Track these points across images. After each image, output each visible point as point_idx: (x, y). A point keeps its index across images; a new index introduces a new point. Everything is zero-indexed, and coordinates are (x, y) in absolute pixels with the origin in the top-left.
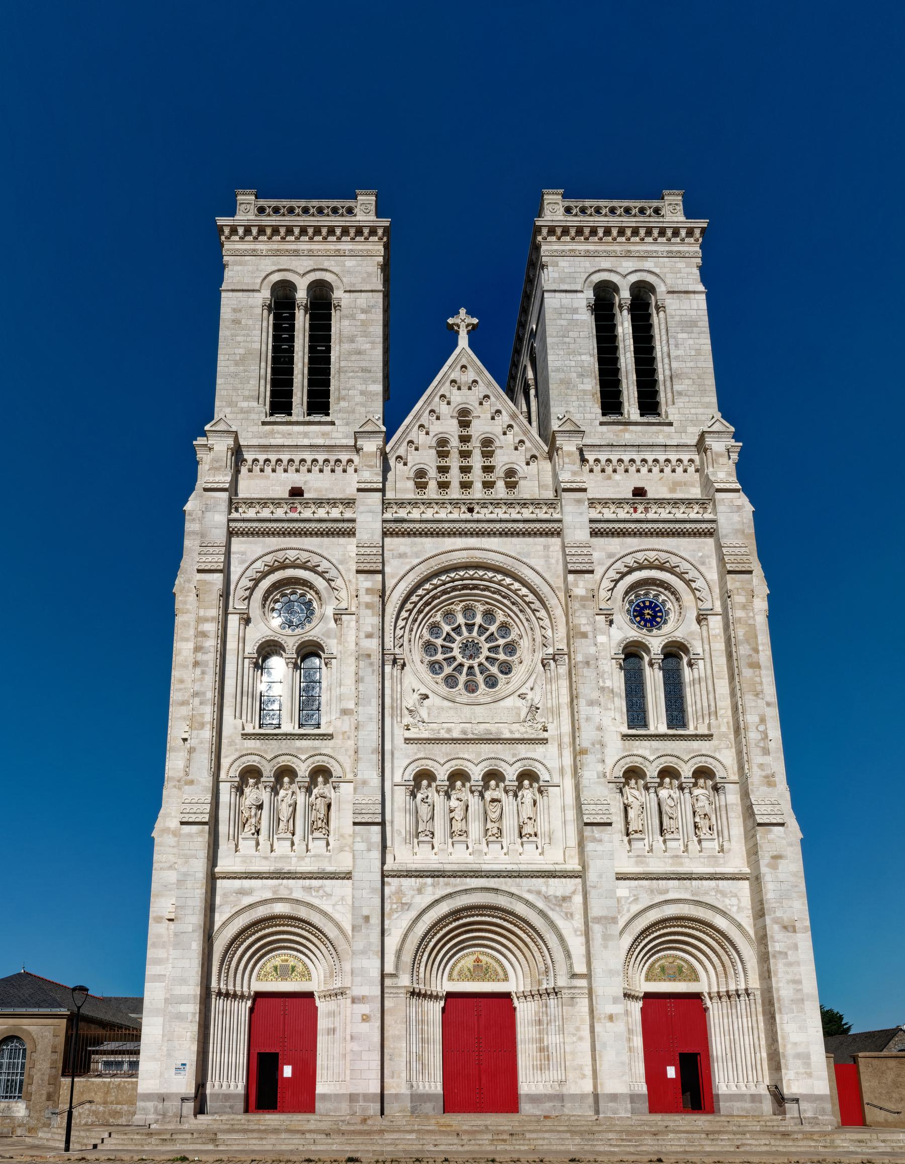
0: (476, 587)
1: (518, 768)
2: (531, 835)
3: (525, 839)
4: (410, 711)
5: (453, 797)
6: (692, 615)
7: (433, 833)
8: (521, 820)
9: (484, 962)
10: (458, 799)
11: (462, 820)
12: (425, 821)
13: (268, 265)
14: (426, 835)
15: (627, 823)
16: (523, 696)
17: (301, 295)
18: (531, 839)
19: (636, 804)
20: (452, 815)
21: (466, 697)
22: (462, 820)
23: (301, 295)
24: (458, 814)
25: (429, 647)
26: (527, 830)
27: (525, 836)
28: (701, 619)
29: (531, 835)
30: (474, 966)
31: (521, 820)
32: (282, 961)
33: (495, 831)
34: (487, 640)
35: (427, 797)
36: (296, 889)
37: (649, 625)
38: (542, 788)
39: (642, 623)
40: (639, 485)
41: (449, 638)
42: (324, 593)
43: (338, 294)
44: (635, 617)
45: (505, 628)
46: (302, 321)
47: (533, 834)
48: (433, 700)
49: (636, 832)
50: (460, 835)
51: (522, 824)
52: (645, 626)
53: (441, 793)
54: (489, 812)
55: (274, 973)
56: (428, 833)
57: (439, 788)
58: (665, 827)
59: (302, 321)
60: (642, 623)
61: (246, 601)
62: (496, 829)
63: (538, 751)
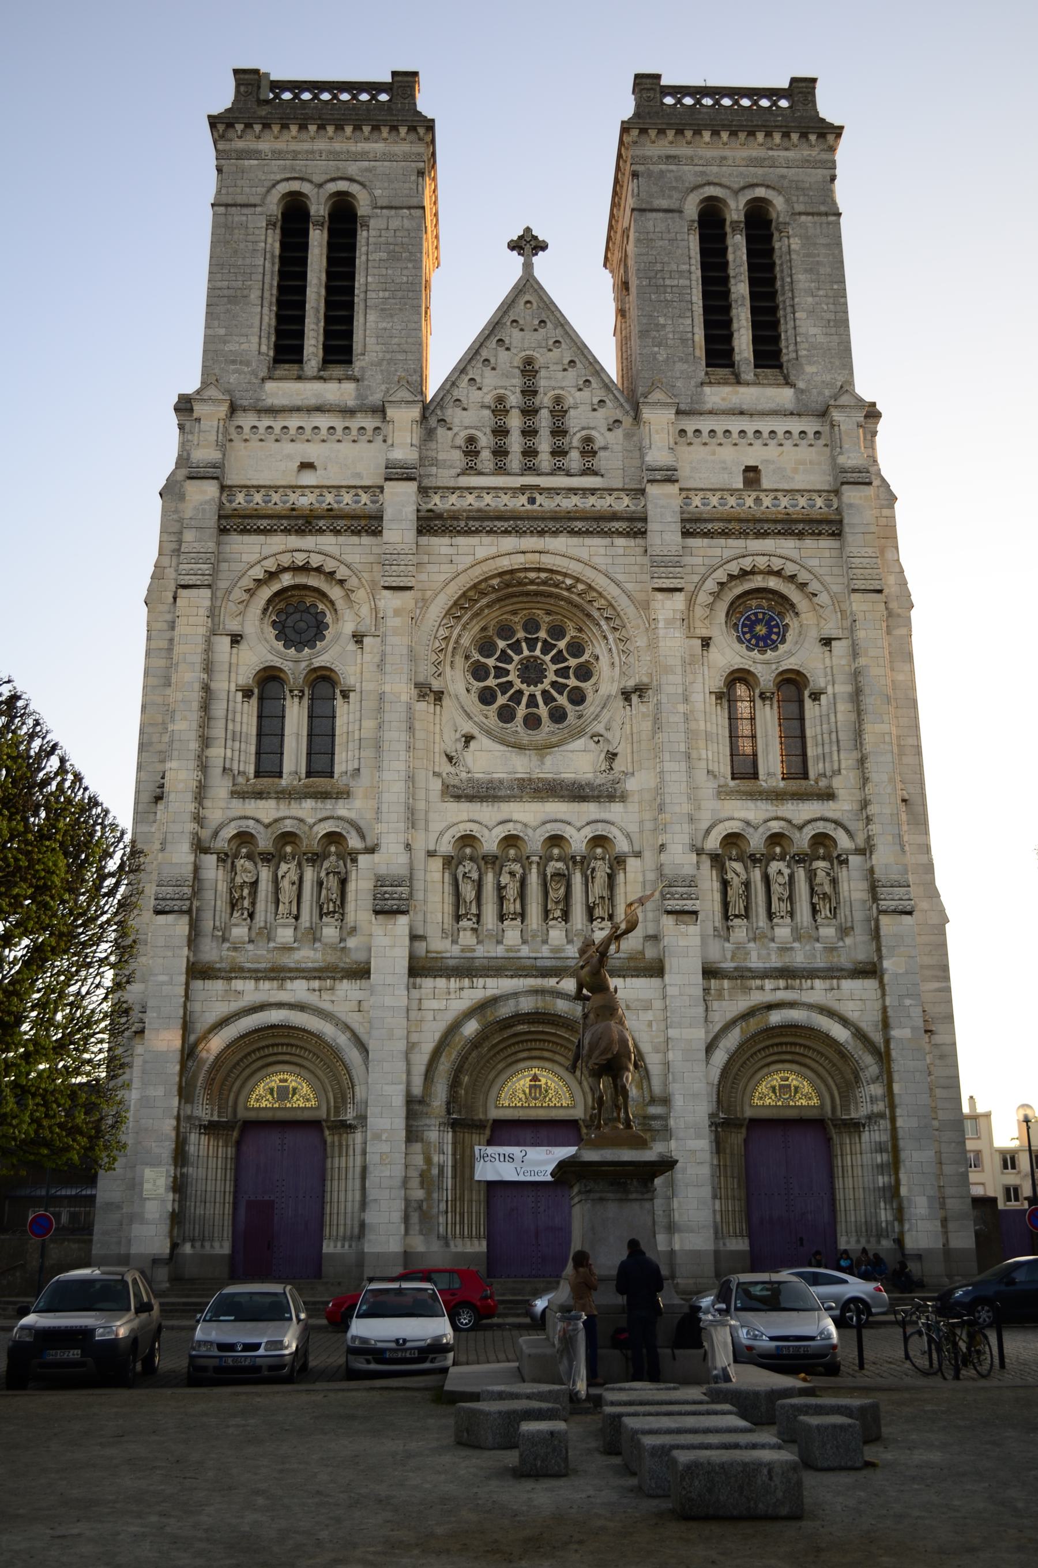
0: (537, 594)
1: (589, 832)
2: (603, 919)
4: (450, 759)
5: (506, 869)
6: (813, 634)
8: (591, 900)
9: (543, 1080)
13: (276, 169)
14: (469, 920)
15: (725, 904)
16: (596, 739)
17: (319, 208)
19: (736, 882)
21: (524, 735)
22: (515, 900)
23: (319, 208)
24: (512, 892)
25: (479, 672)
26: (598, 912)
28: (827, 642)
30: (531, 1087)
32: (281, 1081)
33: (558, 913)
34: (555, 660)
36: (298, 990)
37: (761, 644)
39: (753, 641)
40: (751, 463)
41: (501, 672)
42: (340, 604)
43: (363, 208)
44: (744, 633)
45: (576, 649)
46: (318, 240)
47: (606, 917)
48: (483, 742)
49: (736, 916)
50: (512, 919)
52: (757, 645)
55: (269, 1097)
58: (773, 910)
59: (318, 240)
60: (753, 641)
61: (239, 618)
63: (615, 811)
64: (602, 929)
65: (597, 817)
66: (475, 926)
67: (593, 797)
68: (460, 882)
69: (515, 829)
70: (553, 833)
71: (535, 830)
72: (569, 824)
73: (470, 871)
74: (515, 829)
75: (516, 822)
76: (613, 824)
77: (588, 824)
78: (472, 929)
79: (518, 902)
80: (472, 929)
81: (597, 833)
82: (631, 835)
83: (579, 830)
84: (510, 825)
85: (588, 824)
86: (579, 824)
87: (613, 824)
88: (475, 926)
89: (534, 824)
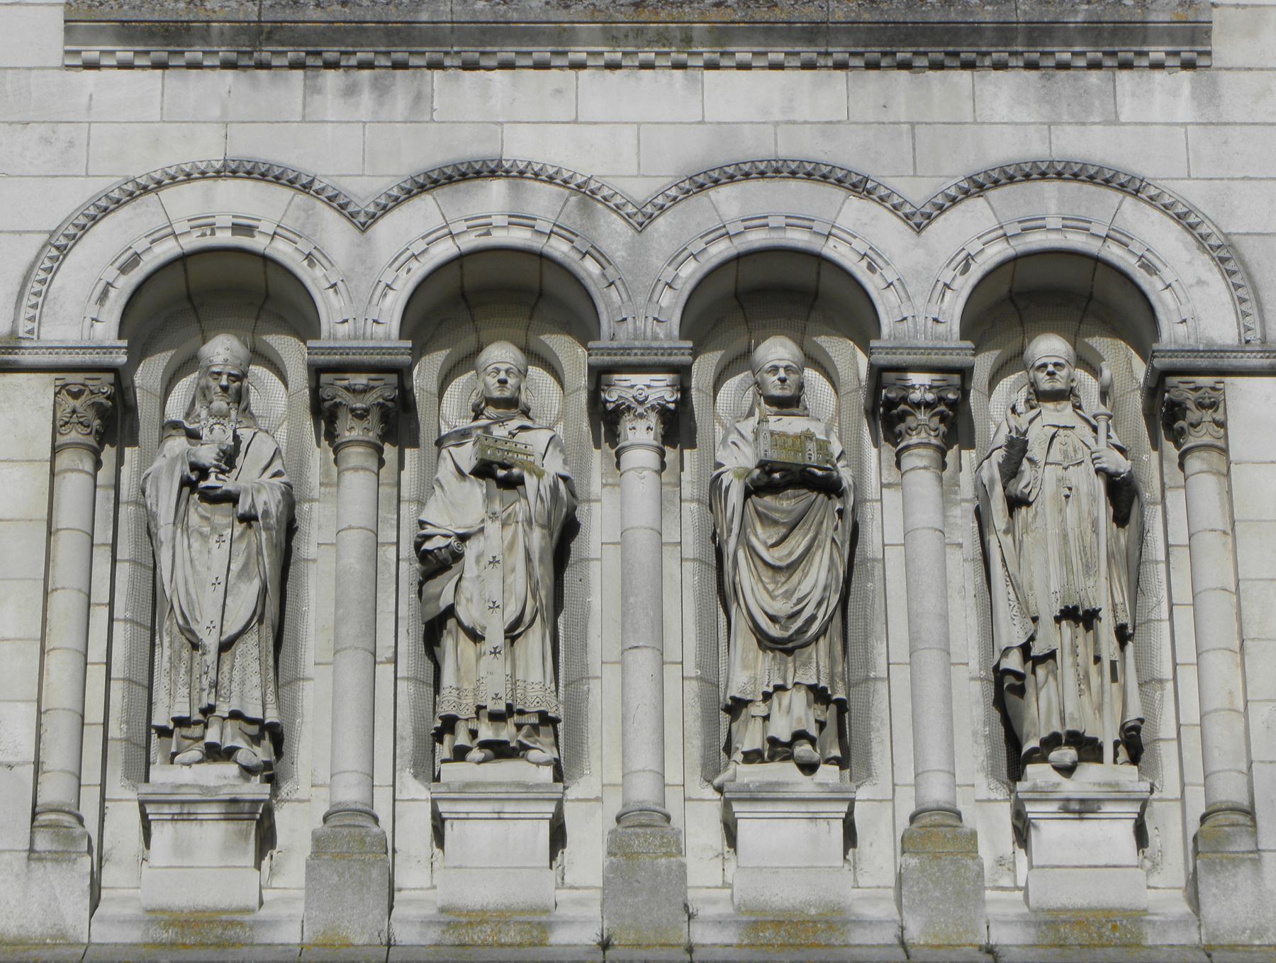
2: (1089, 749)
3: (1037, 773)
7: (275, 735)
10: (484, 470)
11: (513, 633)
12: (211, 641)
14: (215, 753)
18: (1089, 778)
20: (444, 591)
22: (513, 633)
27: (1039, 755)
29: (1089, 749)
31: (1012, 633)
35: (229, 458)
38: (1179, 388)
47: (1108, 735)
50: (499, 750)
51: (1014, 662)
53: (350, 430)
54: (746, 577)
56: (230, 736)
57: (335, 386)
62: (798, 700)
64: (1083, 809)
65: (1035, 148)
66: (256, 789)
67: (1005, 33)
68: (164, 531)
69: (518, 219)
70: (757, 239)
71: (642, 219)
72: (860, 187)
73: (229, 458)
74: (518, 219)
75: (518, 174)
76: (1131, 187)
77: (977, 186)
78: (234, 809)
79: (534, 642)
80: (234, 809)
81: (1037, 241)
82: (1252, 251)
83: (919, 221)
84: (495, 193)
85: (977, 186)
86: (918, 192)
87: (1131, 187)
88: (256, 789)
89: (639, 190)
